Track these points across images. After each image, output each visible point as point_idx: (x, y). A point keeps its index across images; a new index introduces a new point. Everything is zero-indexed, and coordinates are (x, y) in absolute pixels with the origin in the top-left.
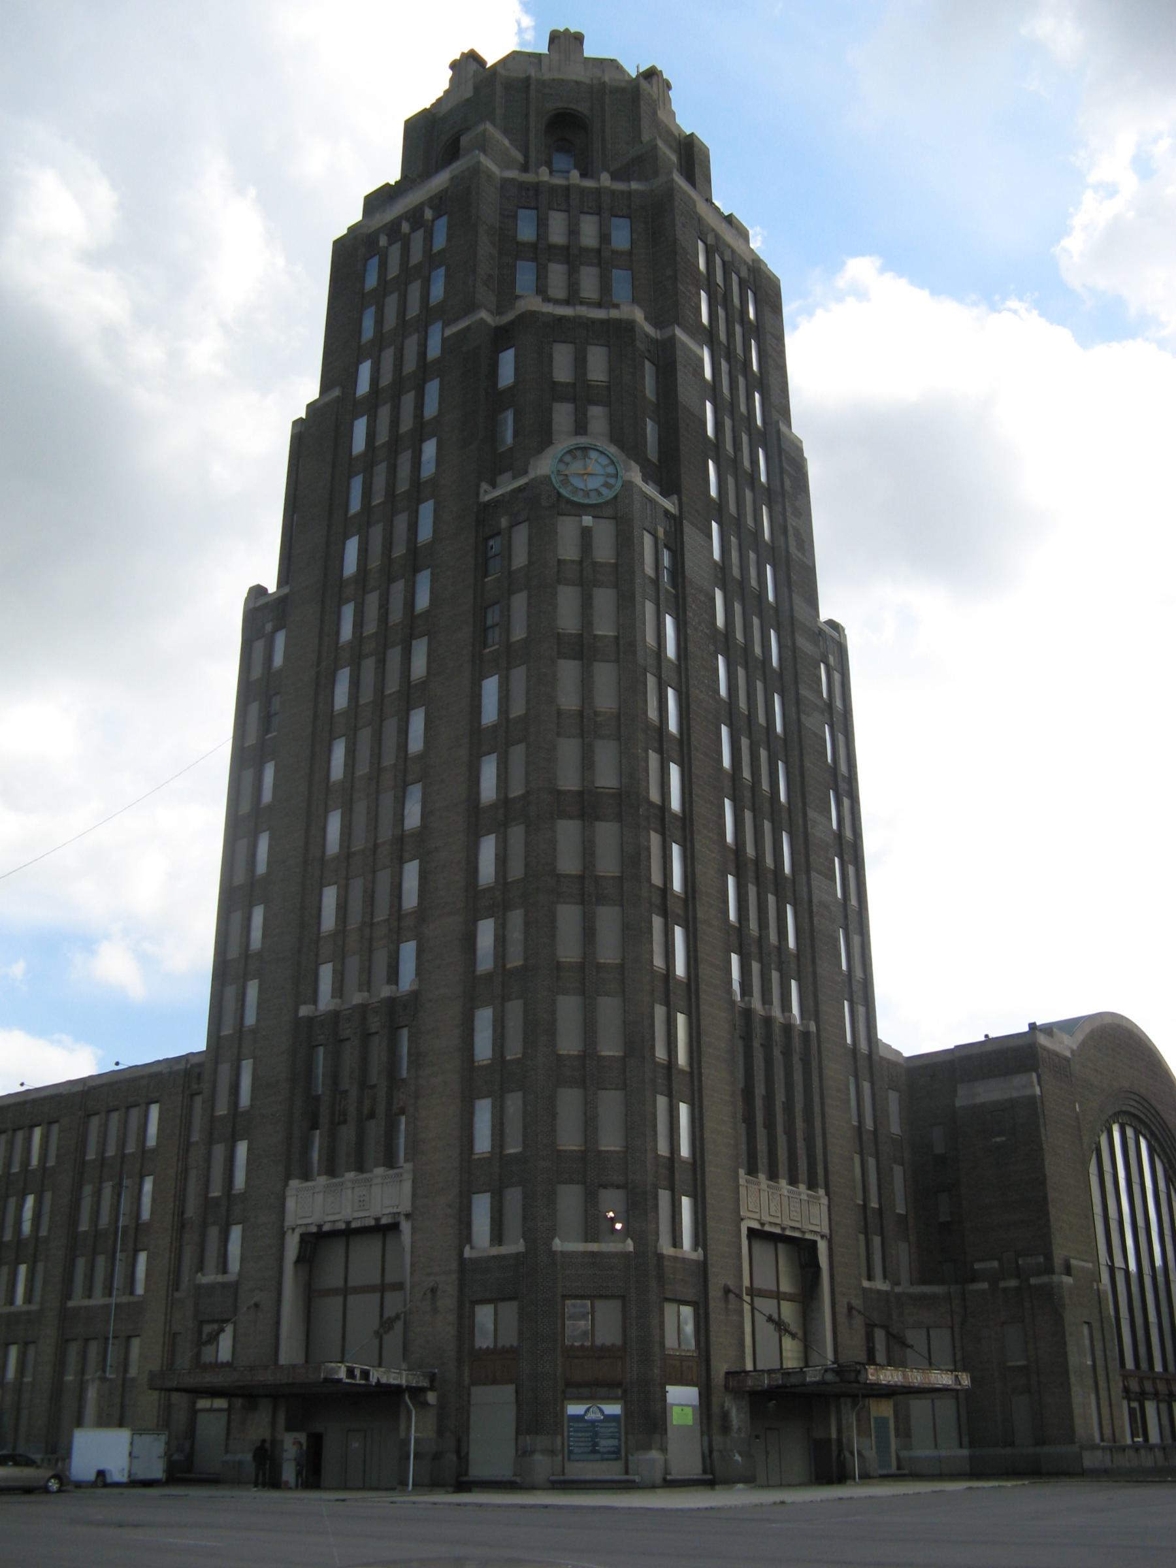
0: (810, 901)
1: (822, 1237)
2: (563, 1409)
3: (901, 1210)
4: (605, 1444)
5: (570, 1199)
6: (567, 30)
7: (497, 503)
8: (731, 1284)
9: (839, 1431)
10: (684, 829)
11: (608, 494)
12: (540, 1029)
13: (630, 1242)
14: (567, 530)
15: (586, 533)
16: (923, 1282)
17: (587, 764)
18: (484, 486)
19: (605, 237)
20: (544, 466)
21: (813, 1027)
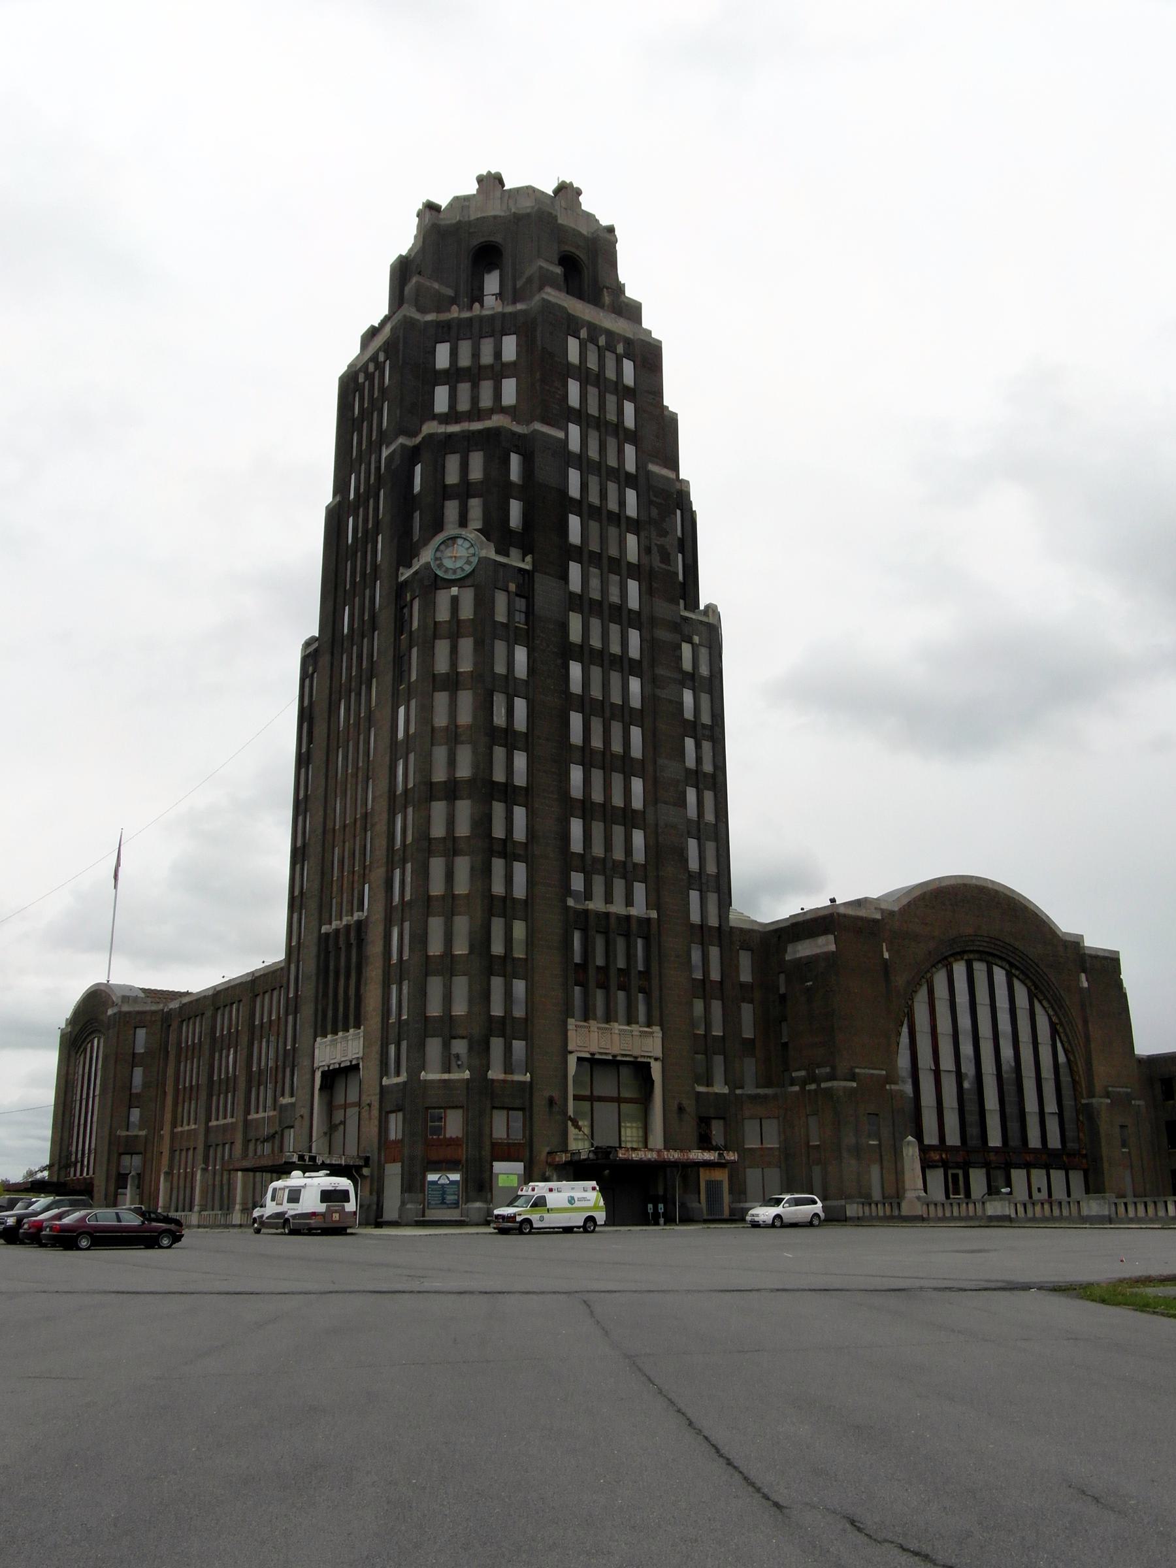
0: (657, 825)
1: (656, 1059)
2: (425, 1177)
3: (748, 1033)
4: (450, 1198)
5: (434, 1047)
6: (489, 172)
7: (406, 582)
8: (556, 1094)
9: (665, 1190)
10: (527, 795)
11: (468, 569)
12: (420, 939)
14: (443, 599)
15: (455, 600)
16: (769, 1084)
17: (452, 763)
18: (401, 570)
19: (498, 354)
20: (426, 556)
21: (654, 914)
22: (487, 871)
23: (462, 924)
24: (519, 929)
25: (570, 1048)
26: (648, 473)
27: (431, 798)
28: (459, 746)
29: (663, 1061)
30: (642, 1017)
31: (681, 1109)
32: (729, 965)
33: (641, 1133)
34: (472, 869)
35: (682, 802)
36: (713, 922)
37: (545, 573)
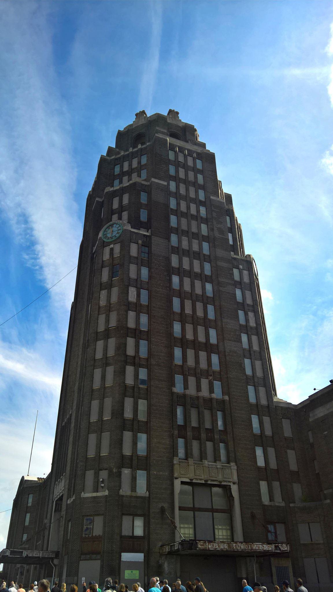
1: (234, 483)
8: (166, 505)
11: (118, 235)
13: (107, 491)
15: (112, 250)
22: (122, 372)
23: (108, 402)
24: (142, 405)
25: (176, 475)
26: (210, 200)
27: (97, 340)
28: (111, 313)
29: (238, 484)
30: (223, 457)
31: (253, 516)
32: (276, 427)
33: (229, 533)
34: (115, 372)
35: (240, 340)
36: (264, 402)
37: (158, 236)
